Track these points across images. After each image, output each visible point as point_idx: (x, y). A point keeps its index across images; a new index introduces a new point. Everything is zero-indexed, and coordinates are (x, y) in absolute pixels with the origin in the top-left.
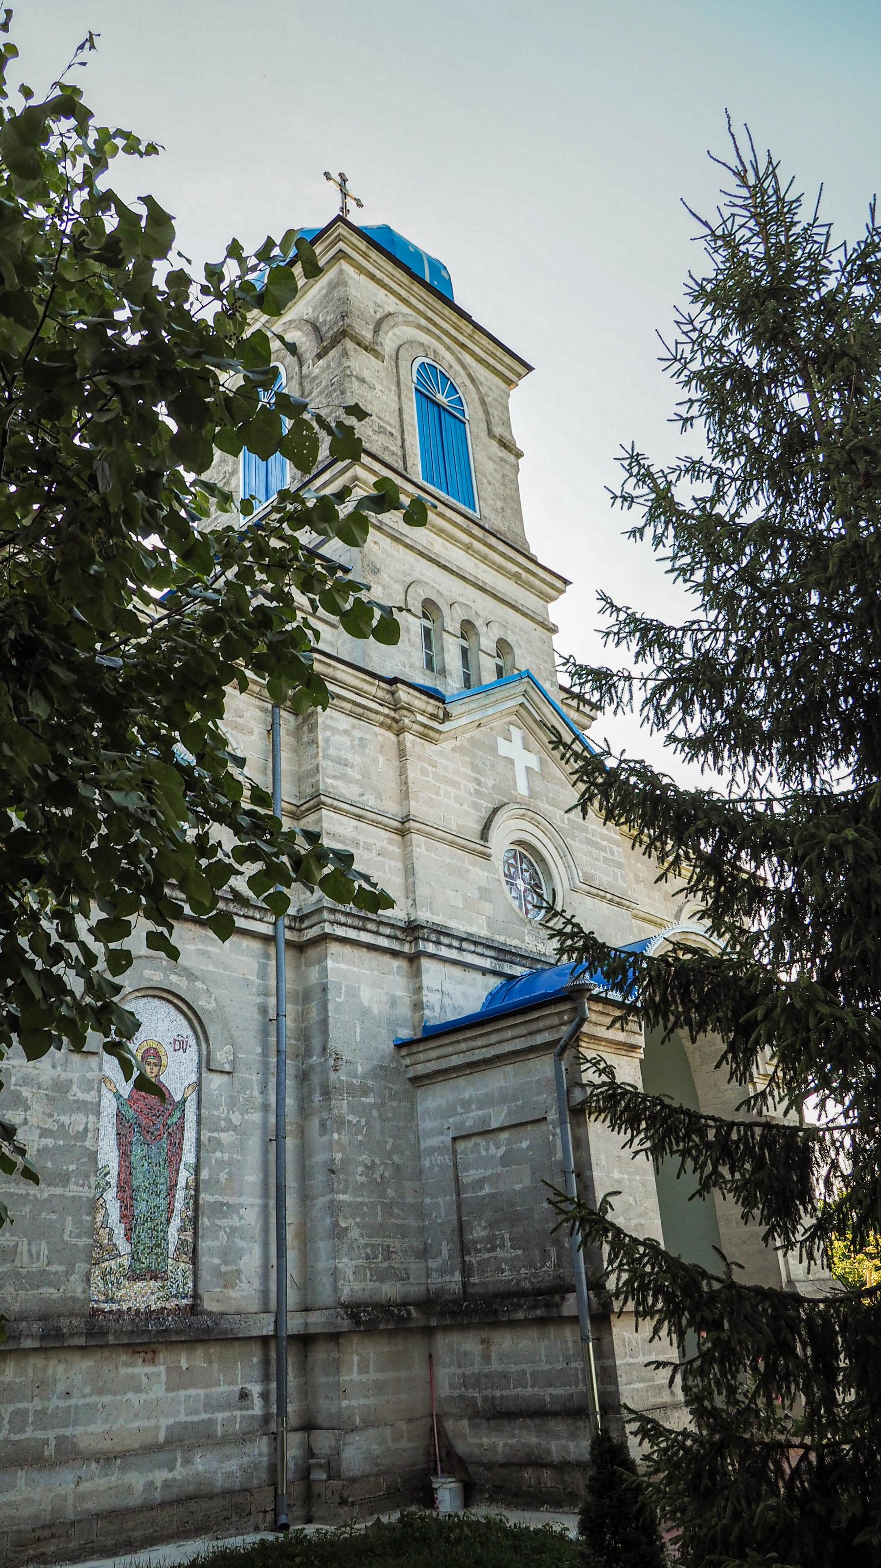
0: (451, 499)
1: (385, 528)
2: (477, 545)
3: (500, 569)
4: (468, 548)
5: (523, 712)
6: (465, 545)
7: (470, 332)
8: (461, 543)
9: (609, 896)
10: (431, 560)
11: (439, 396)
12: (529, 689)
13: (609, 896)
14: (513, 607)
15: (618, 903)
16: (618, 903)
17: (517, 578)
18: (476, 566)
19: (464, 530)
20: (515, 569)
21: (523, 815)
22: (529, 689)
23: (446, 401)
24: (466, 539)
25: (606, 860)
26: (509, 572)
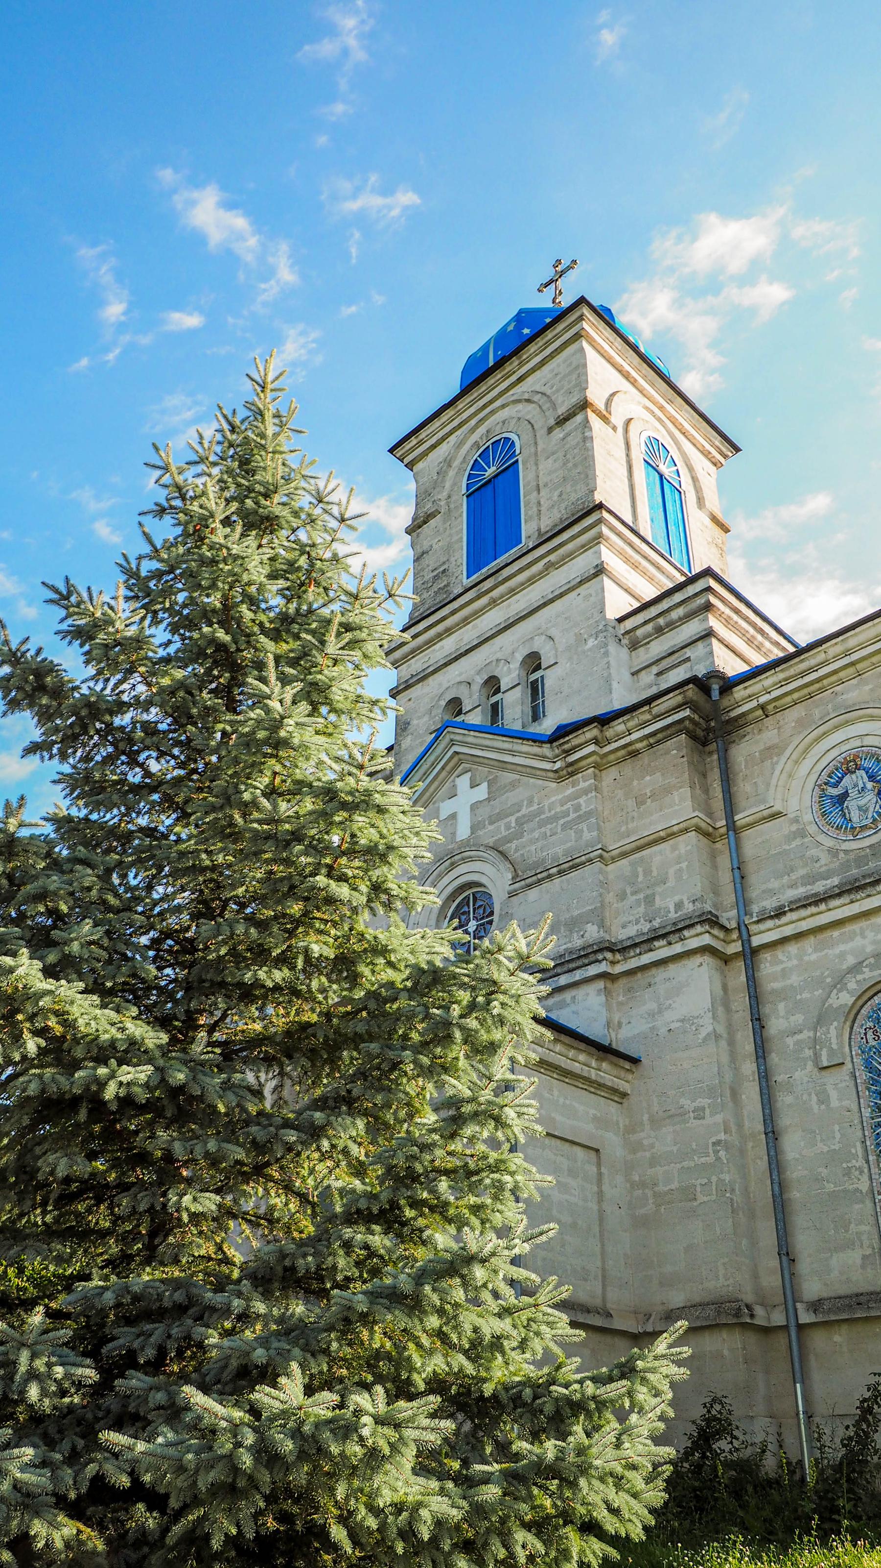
0: (484, 570)
1: (411, 681)
2: (495, 593)
3: (532, 581)
4: (494, 603)
5: (461, 756)
6: (489, 604)
7: (517, 363)
8: (485, 607)
9: (554, 870)
10: (456, 659)
11: (487, 474)
12: (452, 736)
13: (554, 870)
14: (545, 605)
15: (571, 868)
16: (571, 868)
17: (550, 566)
18: (474, 627)
19: (479, 597)
20: (540, 565)
21: (452, 864)
22: (452, 736)
23: (493, 469)
24: (484, 600)
25: (564, 827)
26: (541, 573)
